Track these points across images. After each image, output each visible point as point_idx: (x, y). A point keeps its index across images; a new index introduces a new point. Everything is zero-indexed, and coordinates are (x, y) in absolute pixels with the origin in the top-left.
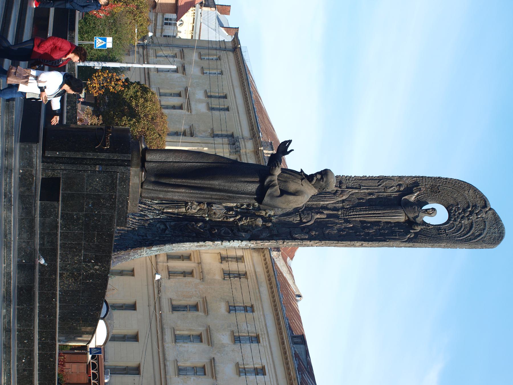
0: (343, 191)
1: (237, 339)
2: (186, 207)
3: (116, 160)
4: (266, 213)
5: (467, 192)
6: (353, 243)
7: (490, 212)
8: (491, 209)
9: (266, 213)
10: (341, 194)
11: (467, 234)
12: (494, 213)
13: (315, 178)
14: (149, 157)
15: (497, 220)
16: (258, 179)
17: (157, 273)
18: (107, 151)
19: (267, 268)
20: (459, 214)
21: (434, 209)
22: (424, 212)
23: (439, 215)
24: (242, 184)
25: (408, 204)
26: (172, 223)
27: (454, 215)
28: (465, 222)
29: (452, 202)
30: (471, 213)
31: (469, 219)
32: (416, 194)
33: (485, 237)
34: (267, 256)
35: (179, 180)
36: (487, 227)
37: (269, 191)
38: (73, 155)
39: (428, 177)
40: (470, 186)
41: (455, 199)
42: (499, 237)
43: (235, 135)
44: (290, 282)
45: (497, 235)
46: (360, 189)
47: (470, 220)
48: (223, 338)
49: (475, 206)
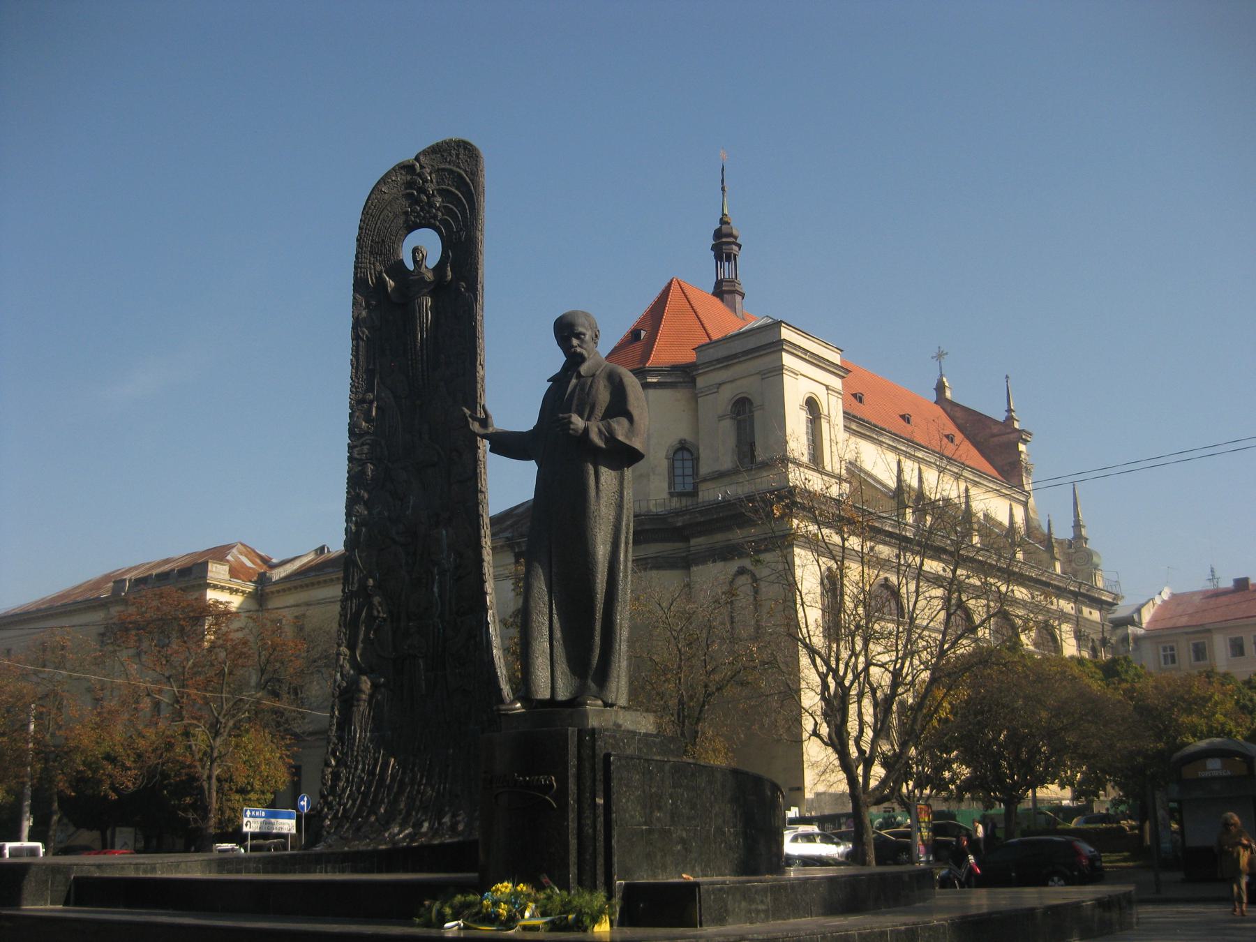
3: (580, 759)
5: (386, 197)
6: (479, 379)
7: (422, 159)
8: (417, 159)
12: (424, 153)
13: (579, 350)
14: (543, 693)
15: (437, 150)
18: (563, 782)
19: (290, 589)
20: (422, 209)
21: (415, 250)
22: (420, 267)
23: (424, 246)
24: (603, 494)
27: (424, 218)
28: (438, 201)
29: (401, 221)
30: (422, 190)
33: (466, 171)
34: (274, 589)
36: (448, 166)
37: (621, 438)
38: (573, 858)
39: (357, 257)
40: (376, 189)
41: (396, 216)
42: (465, 148)
43: (102, 630)
44: (305, 560)
45: (462, 151)
47: (441, 188)
49: (410, 185)
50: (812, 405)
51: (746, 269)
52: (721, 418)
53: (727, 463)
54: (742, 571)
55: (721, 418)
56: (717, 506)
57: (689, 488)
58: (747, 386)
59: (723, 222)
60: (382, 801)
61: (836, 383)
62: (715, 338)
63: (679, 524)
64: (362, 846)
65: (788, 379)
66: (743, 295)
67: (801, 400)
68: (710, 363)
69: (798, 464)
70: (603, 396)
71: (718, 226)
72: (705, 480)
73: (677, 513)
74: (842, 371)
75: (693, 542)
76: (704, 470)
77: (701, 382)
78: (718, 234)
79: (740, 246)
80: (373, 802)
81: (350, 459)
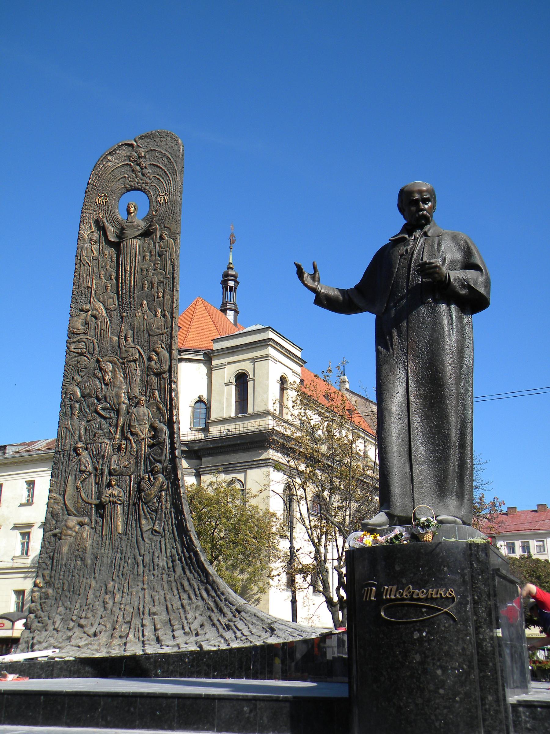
0: (93, 309)
2: (116, 503)
4: (124, 403)
9: (124, 403)
10: (98, 311)
11: (165, 172)
16: (443, 306)
25: (121, 235)
26: (144, 522)
31: (146, 167)
32: (107, 224)
35: (453, 452)
46: (91, 288)
50: (283, 380)
52: (227, 384)
55: (227, 384)
56: (222, 439)
58: (247, 367)
63: (196, 448)
68: (222, 350)
73: (195, 441)
74: (301, 362)
75: (204, 460)
76: (214, 416)
81: (68, 351)
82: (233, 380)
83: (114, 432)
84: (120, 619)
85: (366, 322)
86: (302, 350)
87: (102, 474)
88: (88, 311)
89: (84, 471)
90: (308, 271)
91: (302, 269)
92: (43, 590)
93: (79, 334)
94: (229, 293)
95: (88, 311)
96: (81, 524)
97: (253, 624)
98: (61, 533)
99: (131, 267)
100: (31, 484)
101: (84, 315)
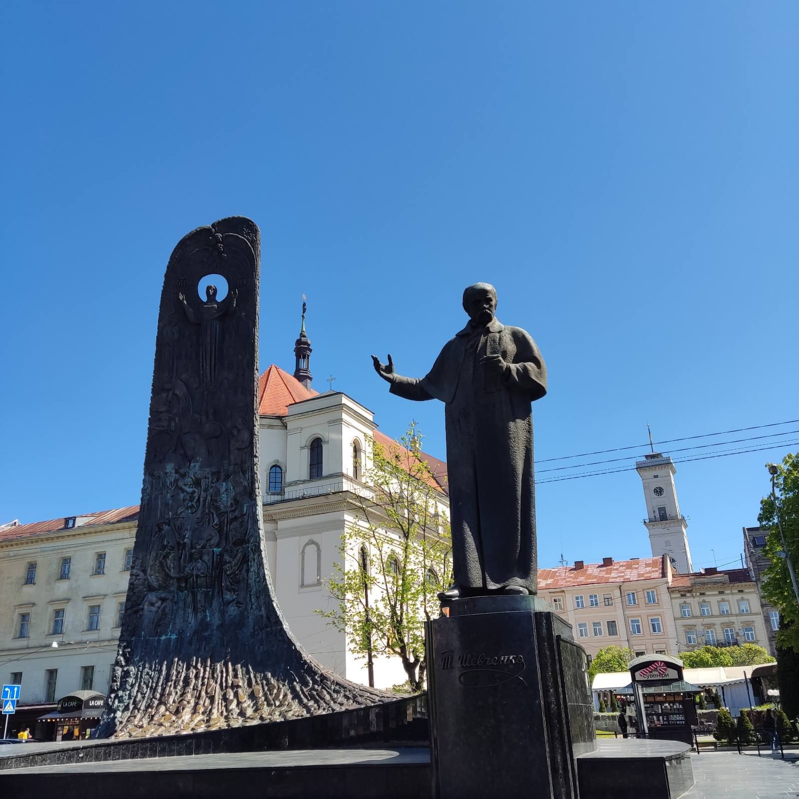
1: (64, 575)
17: (50, 645)
21: (209, 288)
37: (534, 378)
48: (62, 588)
51: (314, 364)
52: (302, 448)
53: (305, 473)
54: (312, 542)
55: (302, 448)
57: (278, 490)
59: (302, 335)
60: (170, 694)
61: (370, 433)
62: (297, 401)
64: (152, 732)
65: (345, 428)
66: (311, 379)
67: (351, 440)
69: (347, 478)
70: (511, 348)
71: (299, 338)
72: (290, 485)
74: (374, 425)
77: (290, 426)
78: (299, 342)
79: (311, 351)
80: (162, 695)
82: (309, 444)
83: (197, 506)
84: (203, 693)
85: (435, 409)
86: (374, 413)
87: (184, 548)
88: (169, 390)
89: (166, 546)
90: (384, 363)
91: (378, 362)
92: (125, 669)
93: (161, 412)
94: (303, 360)
95: (169, 390)
96: (163, 600)
97: (335, 691)
98: (143, 609)
99: (211, 348)
100: (101, 557)
101: (164, 395)
